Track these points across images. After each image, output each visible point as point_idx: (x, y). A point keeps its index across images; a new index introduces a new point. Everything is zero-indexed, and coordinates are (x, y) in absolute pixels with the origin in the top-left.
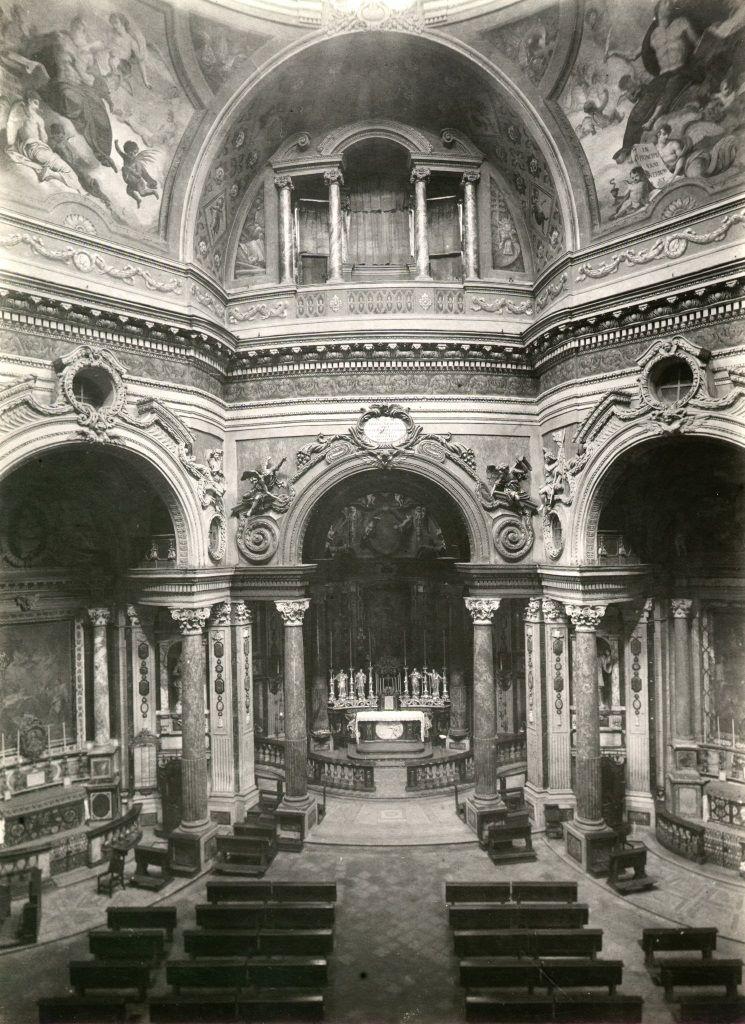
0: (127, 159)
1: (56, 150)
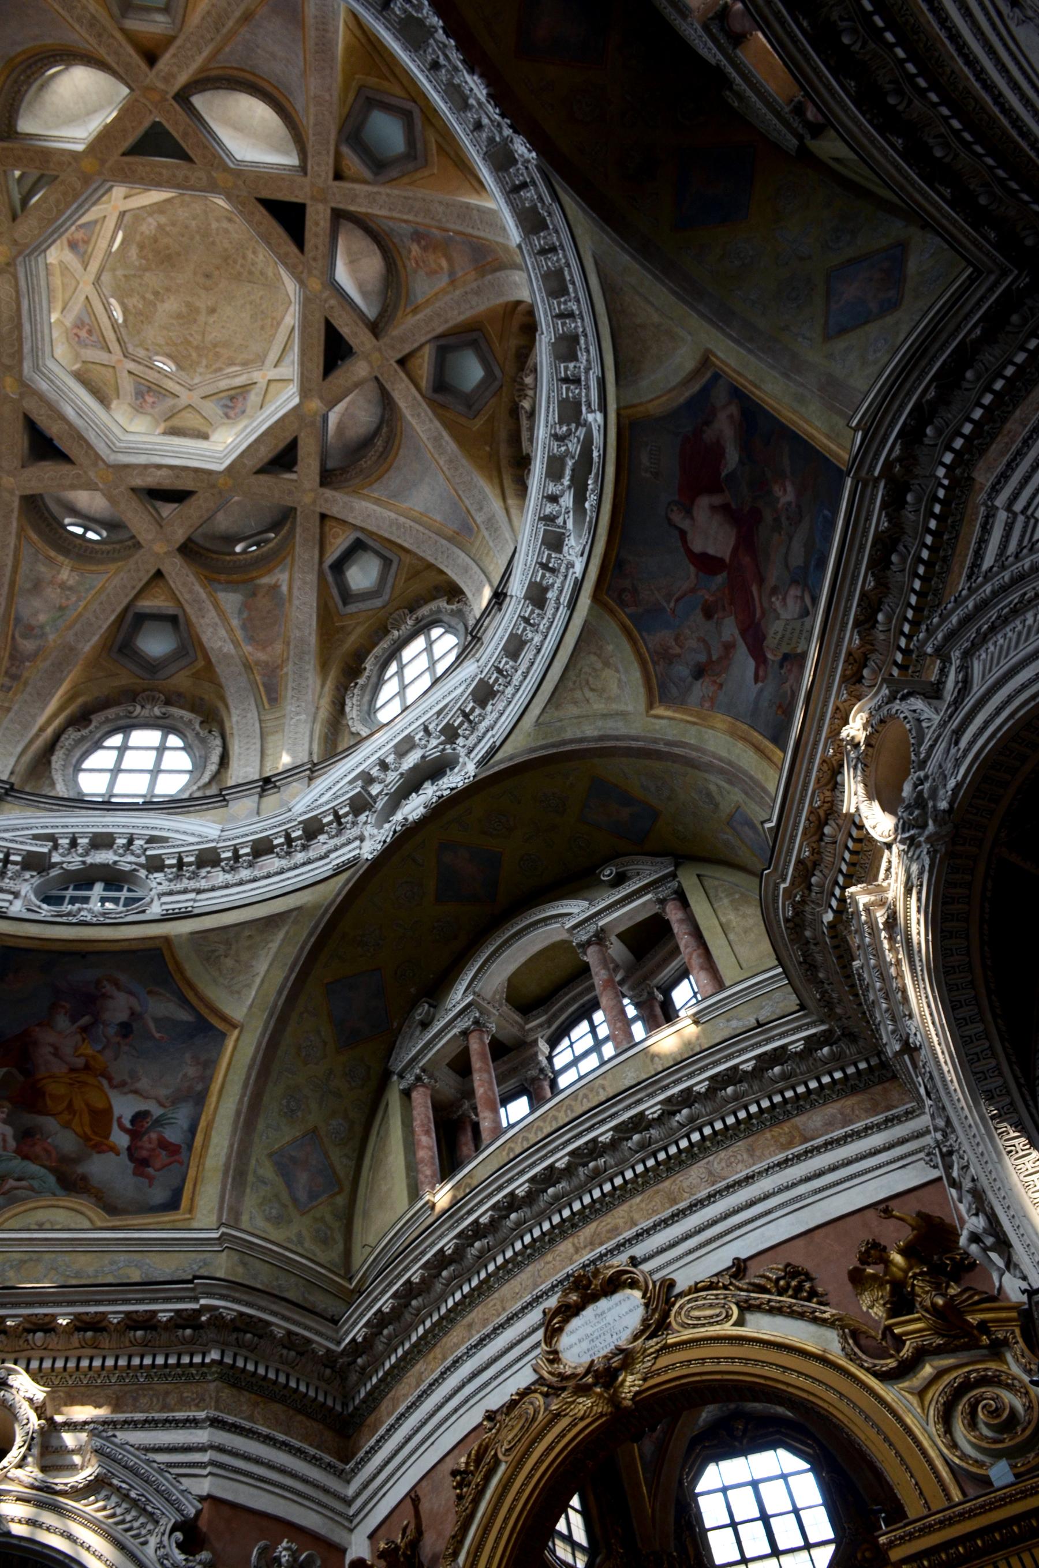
0: (135, 1133)
1: (25, 1157)
